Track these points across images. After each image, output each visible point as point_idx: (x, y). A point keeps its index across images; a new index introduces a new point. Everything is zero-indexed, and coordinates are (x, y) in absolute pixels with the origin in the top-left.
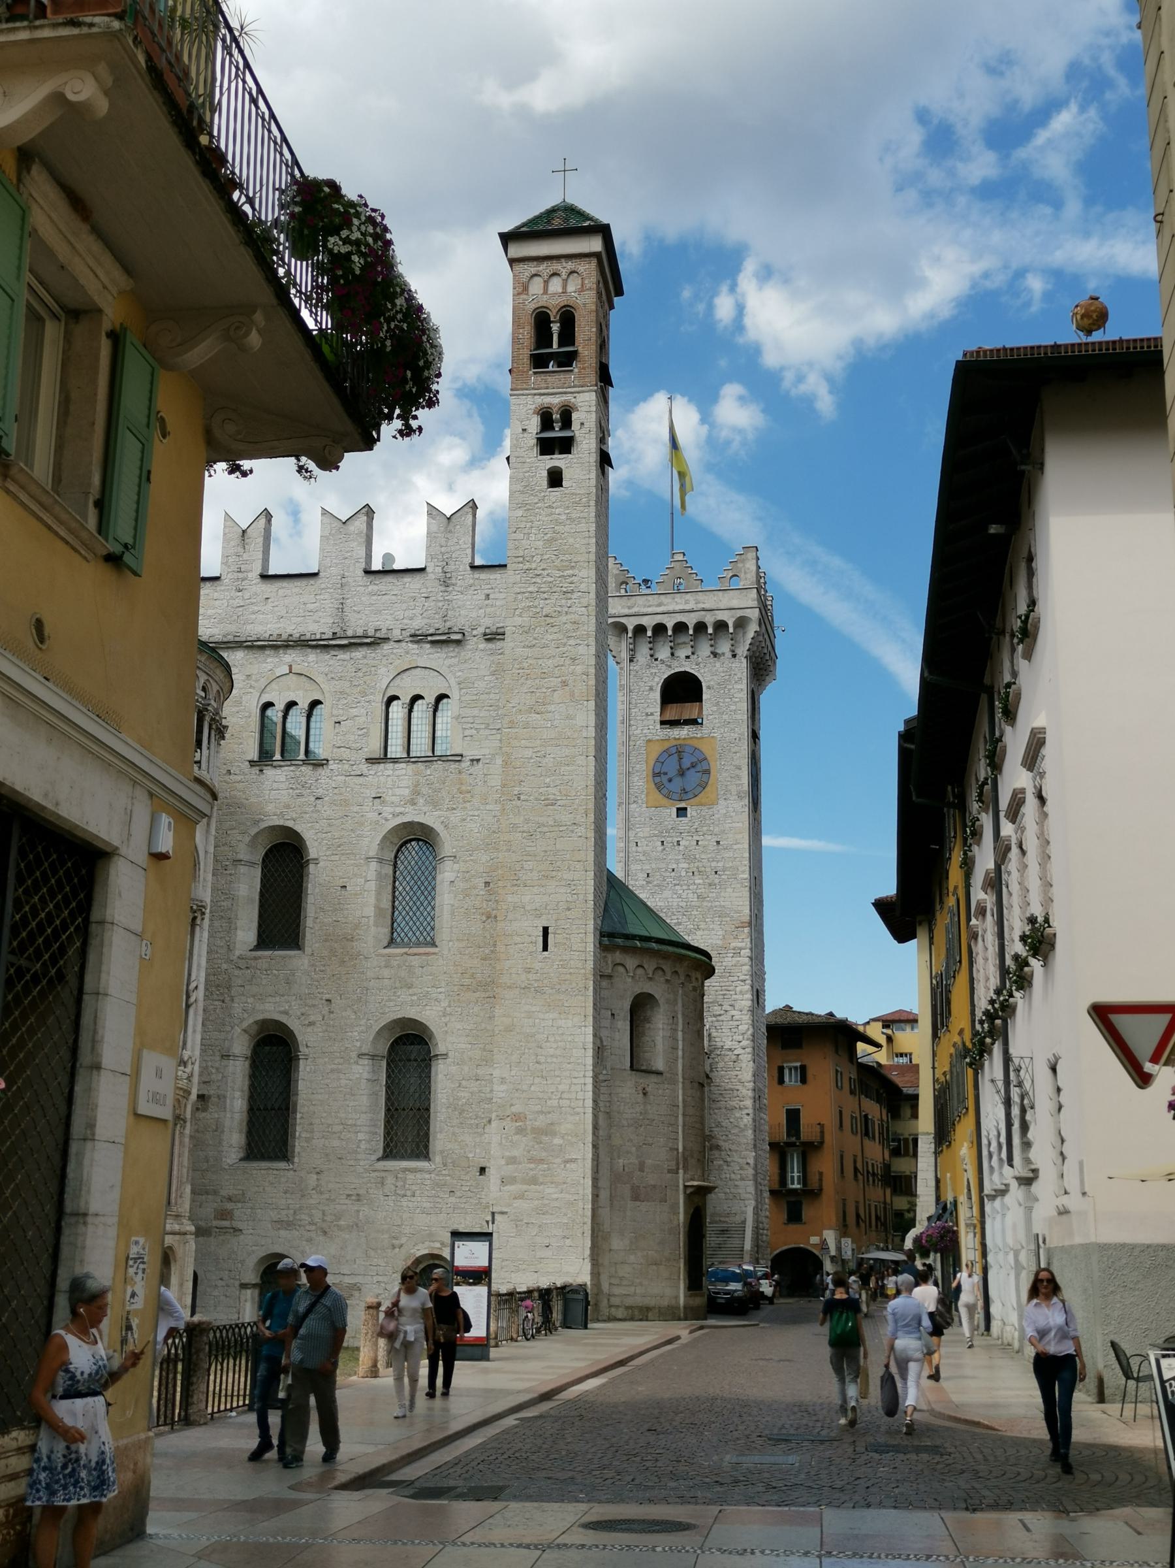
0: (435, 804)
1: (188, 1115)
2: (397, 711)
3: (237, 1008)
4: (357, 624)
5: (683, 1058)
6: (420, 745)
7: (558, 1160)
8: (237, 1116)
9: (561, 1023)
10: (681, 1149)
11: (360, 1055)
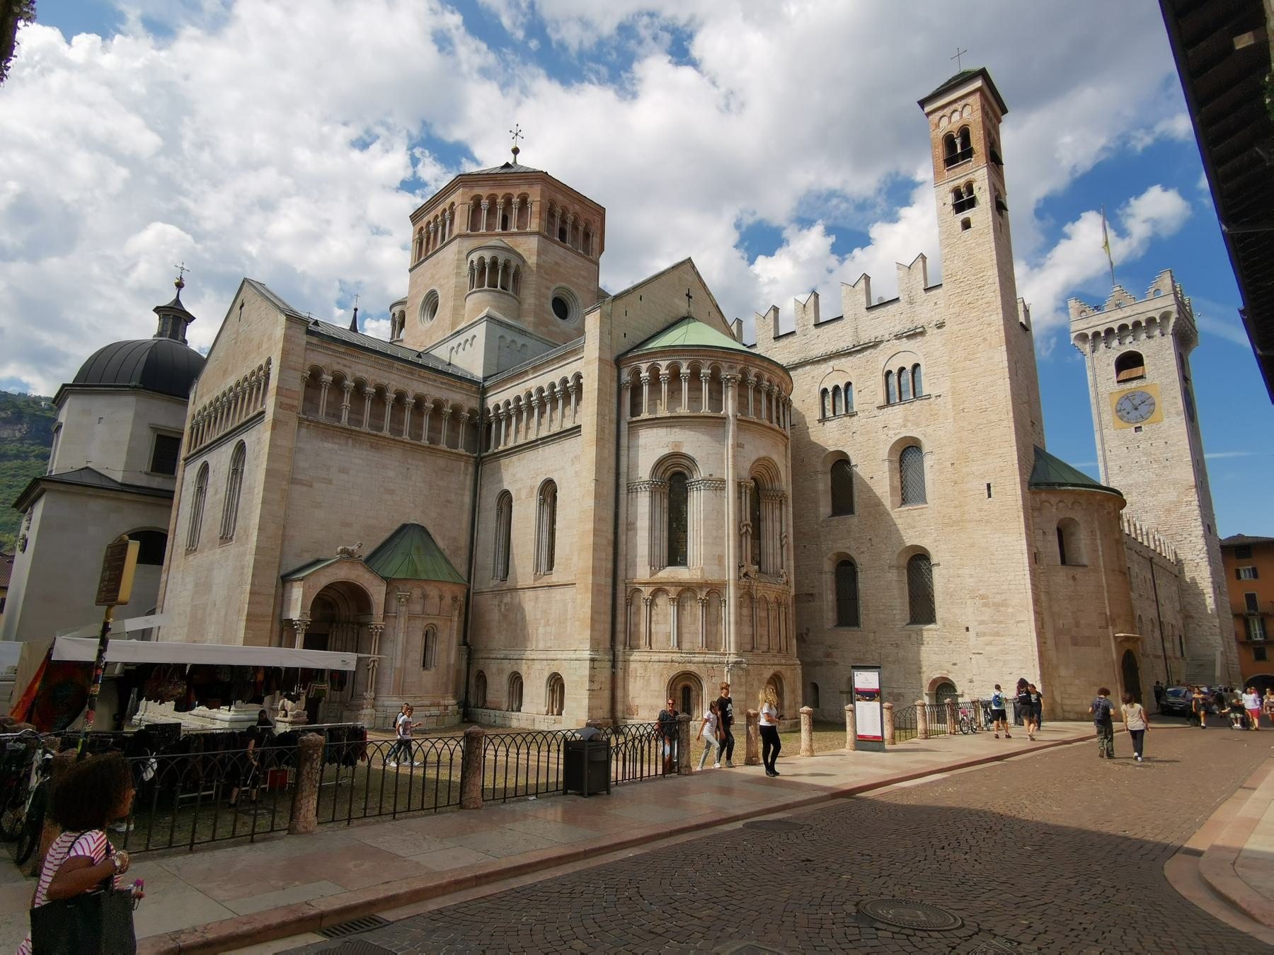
0: (918, 425)
2: (894, 380)
4: (865, 337)
5: (1103, 556)
7: (1012, 622)
10: (1108, 614)
11: (890, 567)
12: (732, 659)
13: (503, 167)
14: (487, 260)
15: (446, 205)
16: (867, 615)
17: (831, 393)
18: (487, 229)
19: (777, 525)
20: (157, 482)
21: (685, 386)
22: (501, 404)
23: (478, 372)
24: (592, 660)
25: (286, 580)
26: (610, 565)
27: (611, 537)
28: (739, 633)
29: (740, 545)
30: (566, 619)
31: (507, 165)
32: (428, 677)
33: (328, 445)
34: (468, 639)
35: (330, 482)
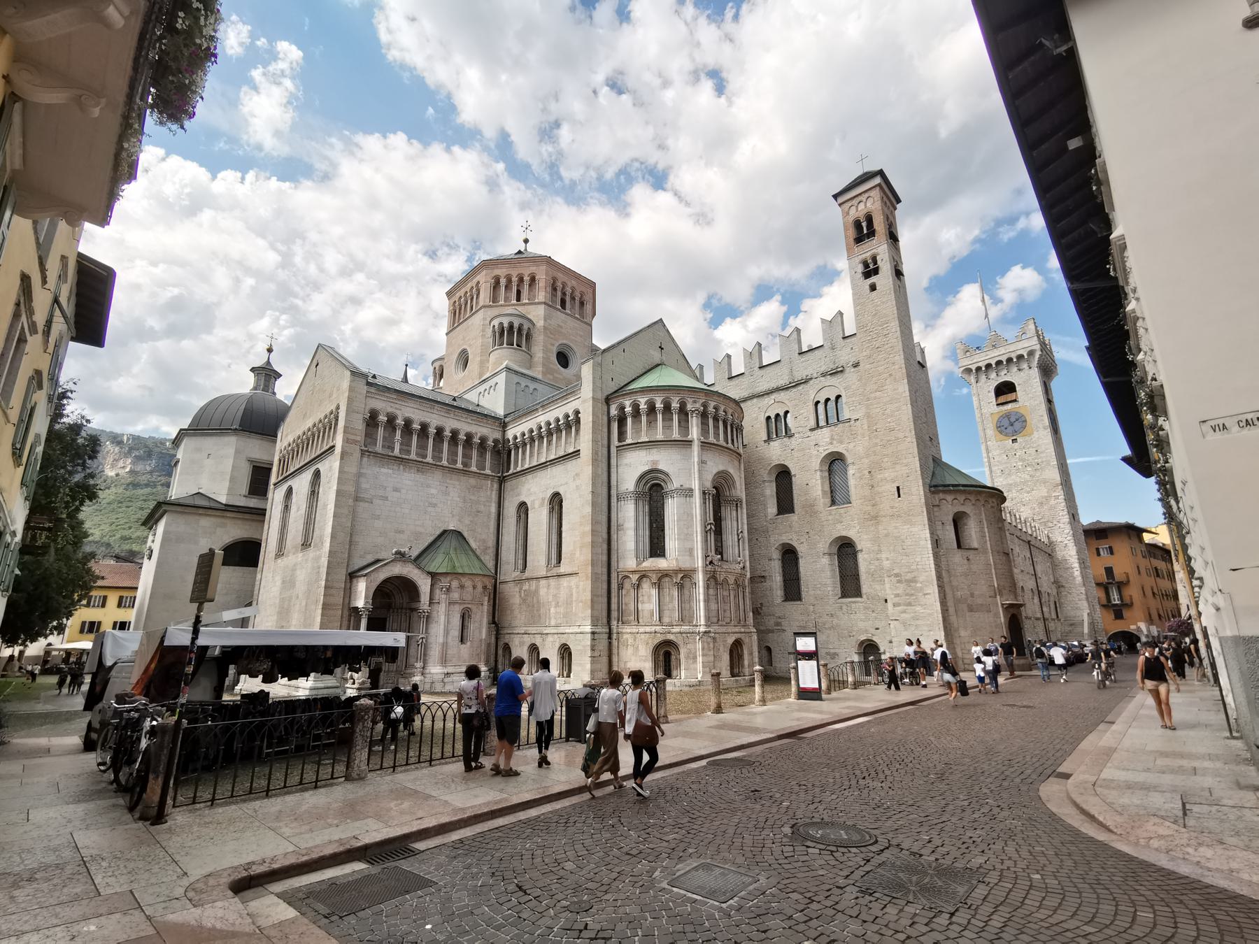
0: (841, 442)
1: (747, 584)
2: (821, 407)
3: (772, 539)
4: (798, 376)
5: (990, 540)
6: (833, 420)
8: (779, 584)
9: (913, 529)
10: (996, 586)
12: (702, 629)
13: (516, 254)
14: (506, 325)
15: (473, 283)
16: (807, 592)
17: (773, 420)
18: (505, 301)
19: (735, 523)
20: (253, 503)
21: (660, 417)
22: (518, 435)
23: (500, 411)
24: (593, 633)
25: (352, 576)
26: (605, 558)
27: (605, 536)
28: (707, 609)
29: (706, 541)
30: (572, 601)
31: (520, 252)
32: (465, 649)
33: (384, 470)
34: (496, 619)
35: (386, 499)
